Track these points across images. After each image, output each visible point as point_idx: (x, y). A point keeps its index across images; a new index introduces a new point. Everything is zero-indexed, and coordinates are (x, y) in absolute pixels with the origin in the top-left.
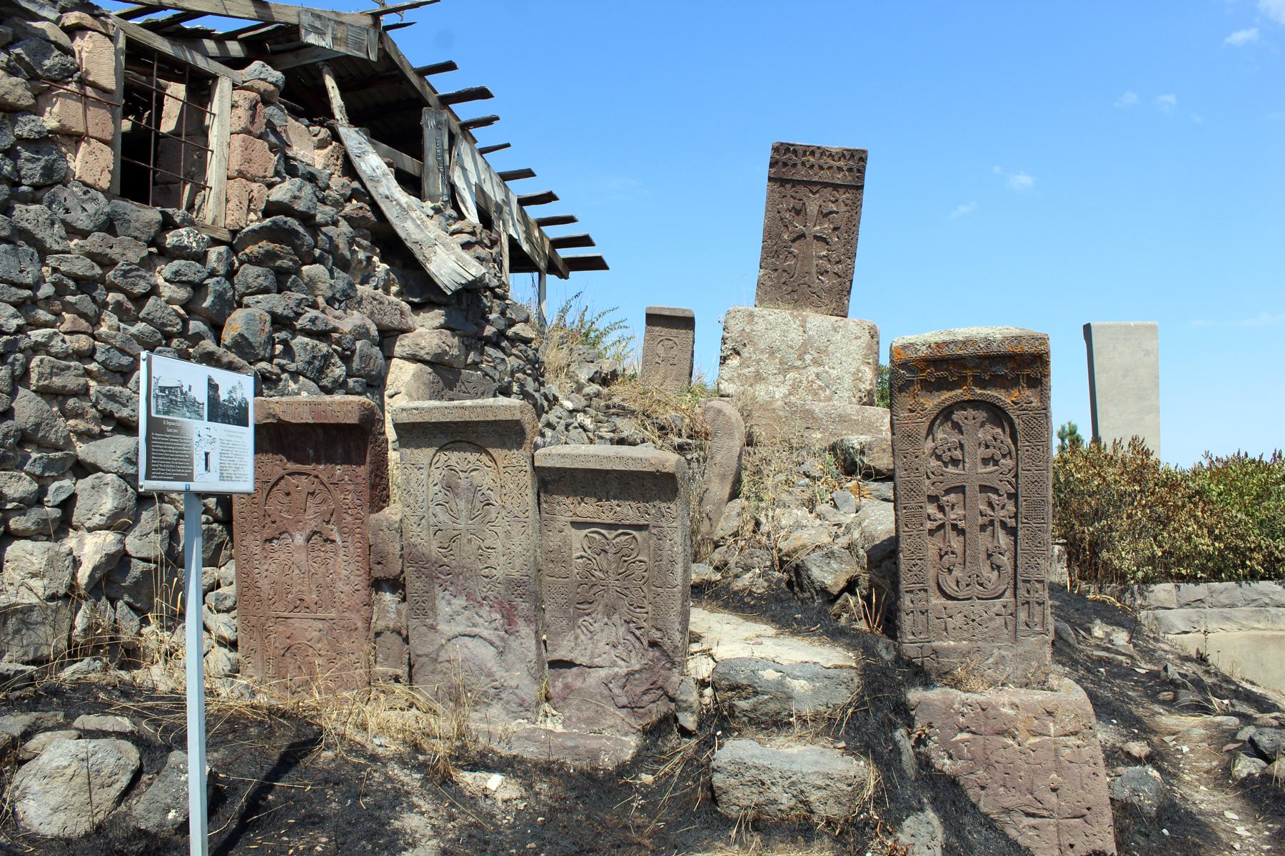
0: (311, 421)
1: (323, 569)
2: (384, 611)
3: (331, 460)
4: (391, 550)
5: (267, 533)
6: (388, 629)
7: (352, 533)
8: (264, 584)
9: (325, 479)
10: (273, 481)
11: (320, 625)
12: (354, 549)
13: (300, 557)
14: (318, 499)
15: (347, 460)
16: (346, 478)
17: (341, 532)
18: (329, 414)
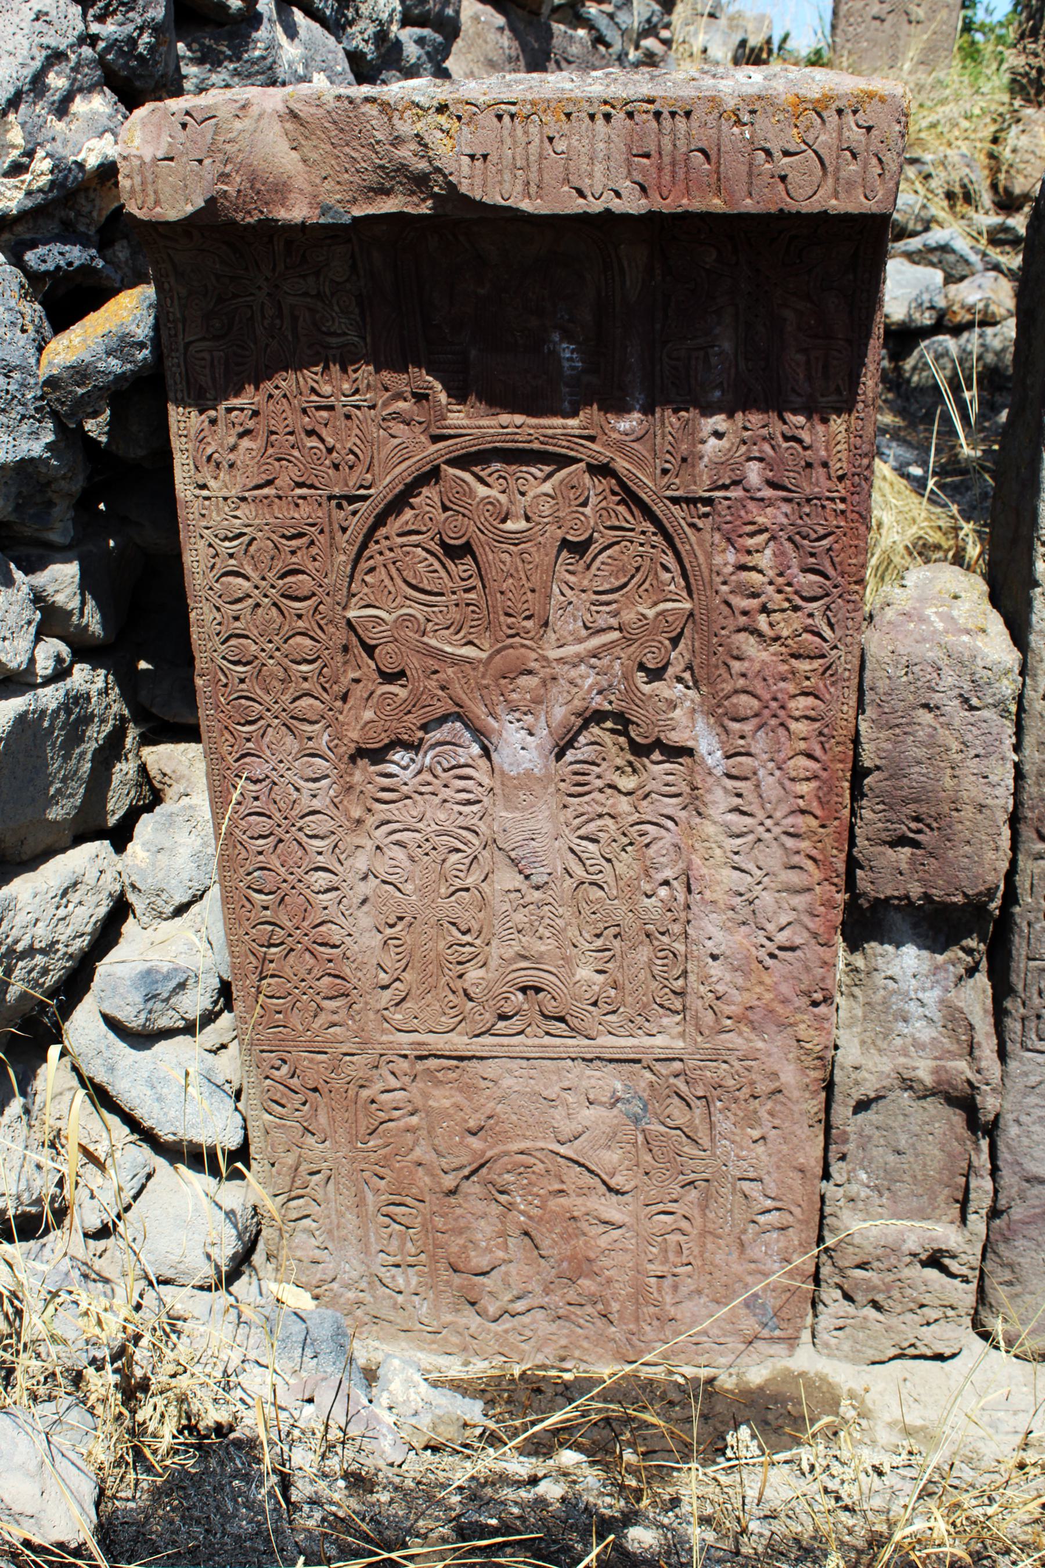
0: (632, 204)
1: (626, 864)
2: (884, 1016)
3: (676, 389)
4: (972, 789)
5: (361, 721)
6: (907, 1084)
7: (773, 715)
8: (362, 937)
9: (647, 484)
10: (383, 489)
11: (610, 1081)
12: (785, 776)
13: (540, 826)
14: (603, 569)
15: (759, 389)
16: (754, 473)
17: (722, 715)
18: (734, 167)
